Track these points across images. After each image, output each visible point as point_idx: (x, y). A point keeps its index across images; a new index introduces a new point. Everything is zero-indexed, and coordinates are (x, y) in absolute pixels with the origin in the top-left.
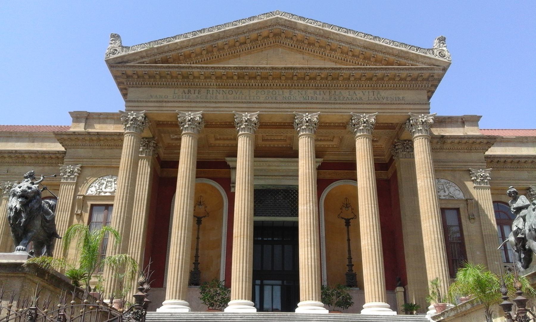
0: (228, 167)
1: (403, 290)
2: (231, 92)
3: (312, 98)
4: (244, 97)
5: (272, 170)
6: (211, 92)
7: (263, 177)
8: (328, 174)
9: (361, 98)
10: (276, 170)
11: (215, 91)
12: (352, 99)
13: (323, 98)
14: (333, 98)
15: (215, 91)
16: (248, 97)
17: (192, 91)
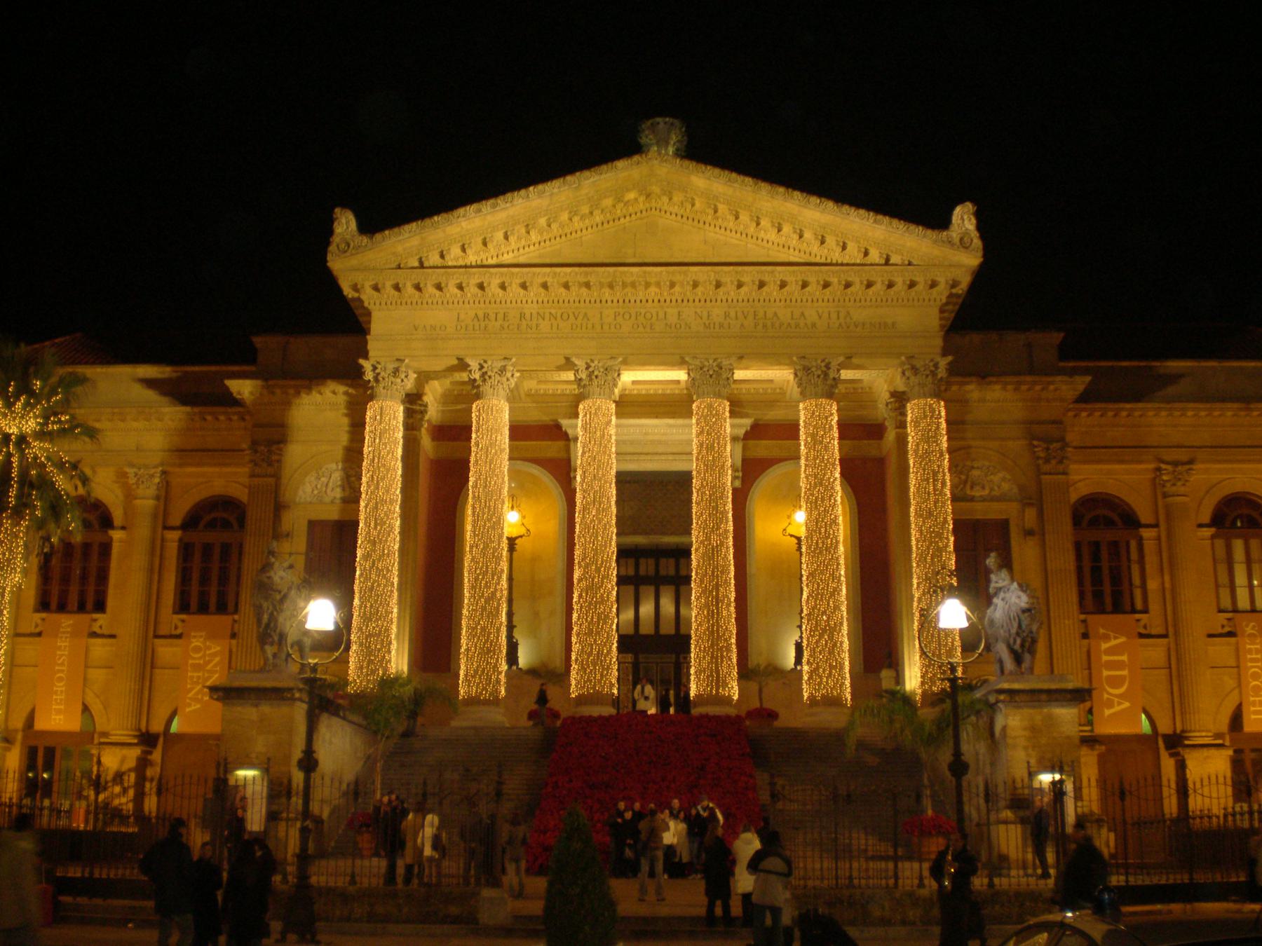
0: (565, 437)
1: (894, 674)
2: (565, 316)
3: (721, 326)
4: (590, 326)
5: (652, 442)
6: (528, 316)
7: (635, 457)
8: (763, 448)
9: (814, 325)
10: (660, 442)
11: (535, 315)
12: (797, 326)
13: (742, 325)
14: (760, 327)
15: (535, 315)
16: (598, 327)
17: (492, 316)
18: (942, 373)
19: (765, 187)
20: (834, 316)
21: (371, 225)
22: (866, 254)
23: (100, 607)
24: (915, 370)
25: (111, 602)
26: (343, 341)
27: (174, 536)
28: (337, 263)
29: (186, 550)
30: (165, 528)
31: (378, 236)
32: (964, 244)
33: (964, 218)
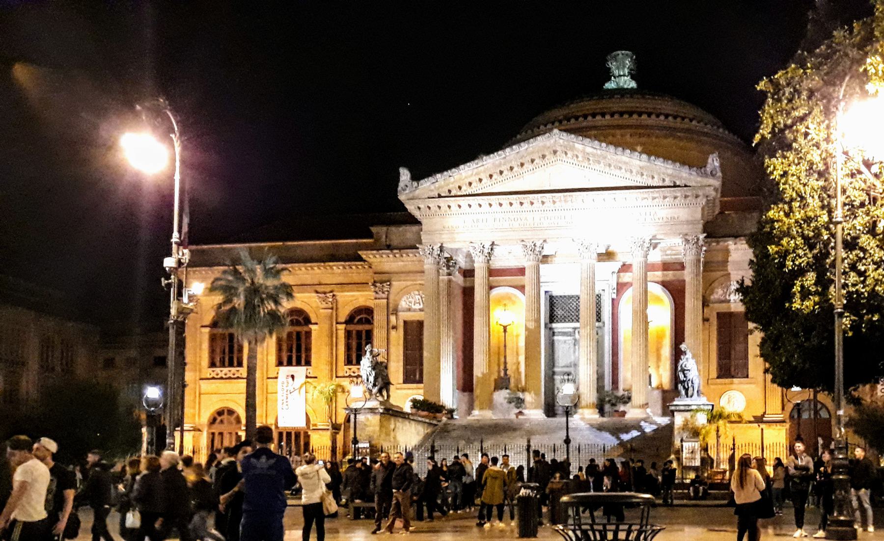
18: (701, 242)
19: (612, 148)
20: (648, 214)
21: (417, 177)
22: (664, 180)
23: (308, 363)
24: (687, 241)
25: (313, 360)
26: (415, 228)
27: (342, 327)
28: (402, 197)
29: (348, 334)
30: (337, 323)
31: (422, 181)
32: (713, 175)
33: (714, 162)
